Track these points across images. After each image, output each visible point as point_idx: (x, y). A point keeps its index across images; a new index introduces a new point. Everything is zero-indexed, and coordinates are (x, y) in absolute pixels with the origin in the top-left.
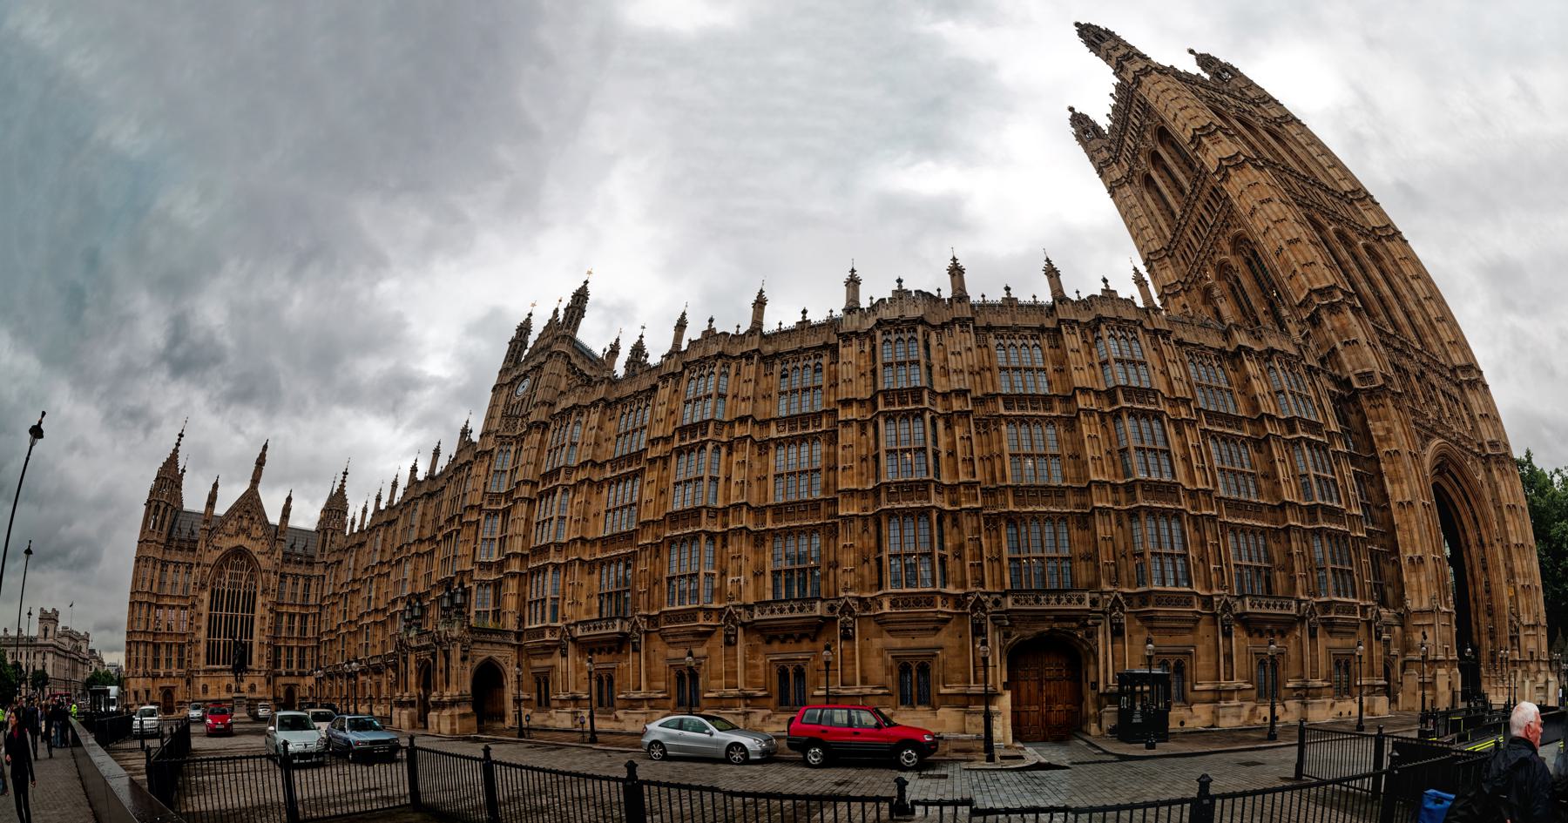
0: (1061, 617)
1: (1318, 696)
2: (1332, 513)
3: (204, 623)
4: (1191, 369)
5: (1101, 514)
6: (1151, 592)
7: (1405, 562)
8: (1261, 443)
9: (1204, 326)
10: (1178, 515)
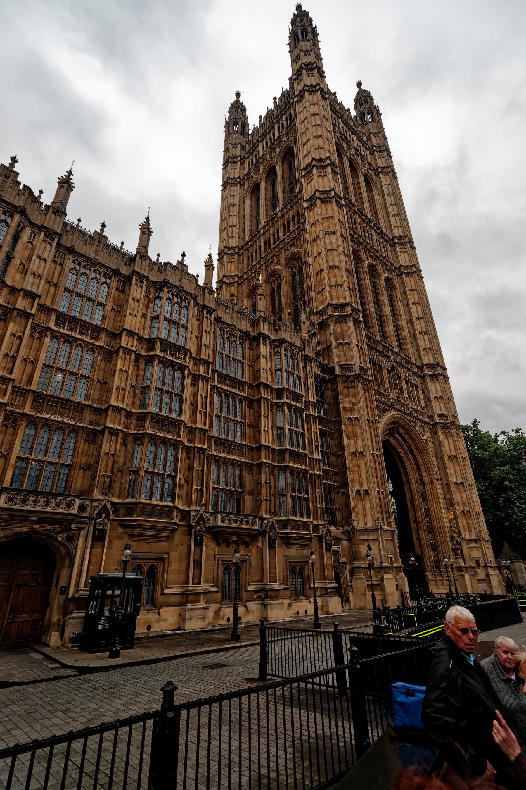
0: (45, 519)
1: (276, 598)
2: (296, 456)
4: (219, 341)
5: (110, 433)
6: (137, 504)
7: (352, 494)
8: (253, 403)
9: (241, 313)
10: (175, 444)
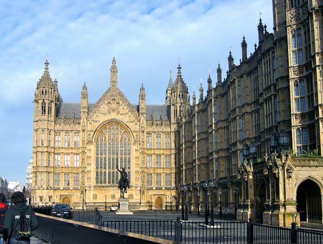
3: (93, 162)
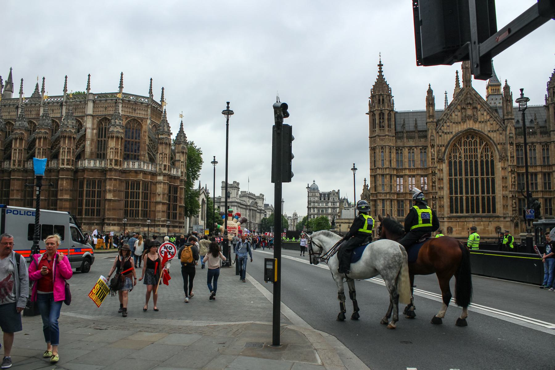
3: (446, 184)
